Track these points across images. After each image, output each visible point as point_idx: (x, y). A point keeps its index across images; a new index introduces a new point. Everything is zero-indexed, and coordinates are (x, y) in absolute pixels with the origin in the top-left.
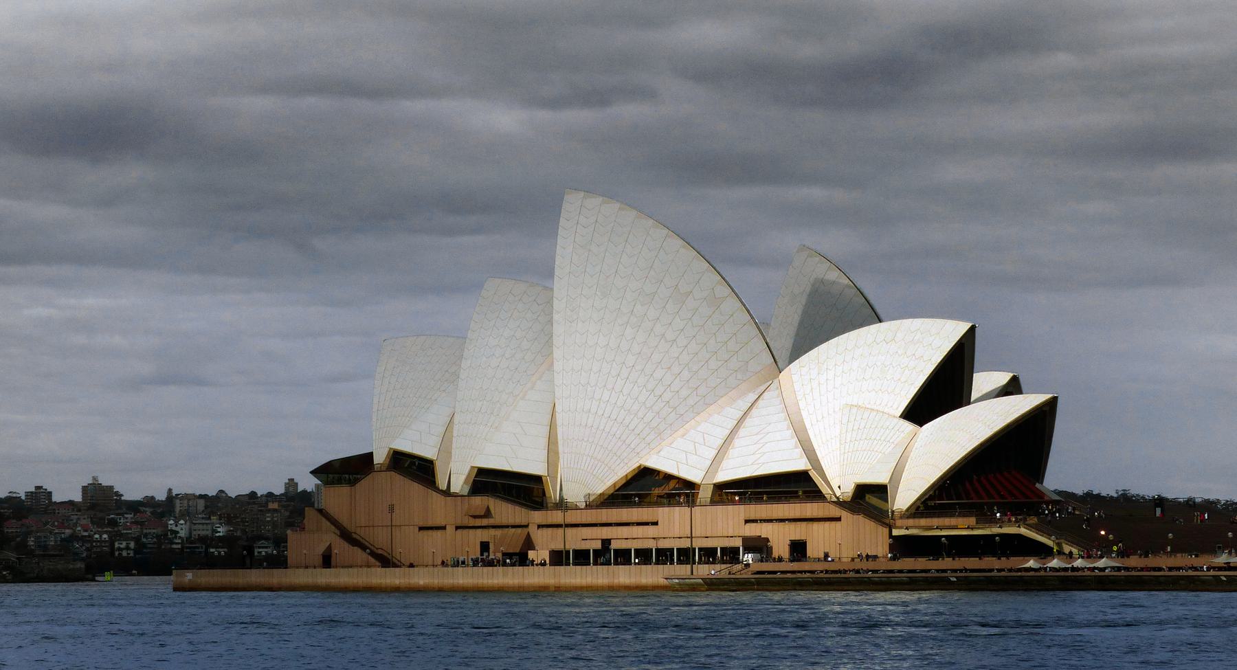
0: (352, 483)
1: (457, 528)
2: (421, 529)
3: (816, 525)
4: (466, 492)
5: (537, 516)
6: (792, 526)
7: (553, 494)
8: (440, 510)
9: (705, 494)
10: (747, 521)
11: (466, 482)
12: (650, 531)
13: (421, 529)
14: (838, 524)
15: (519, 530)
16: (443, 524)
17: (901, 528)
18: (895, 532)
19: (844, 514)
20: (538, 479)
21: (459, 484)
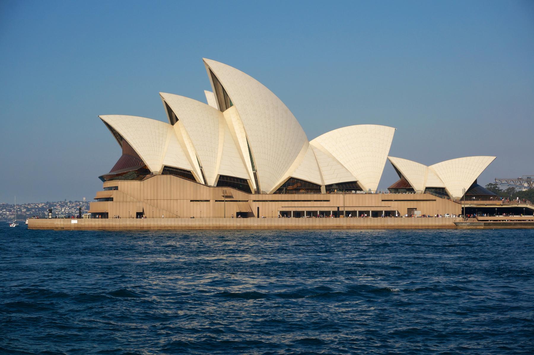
0: (141, 179)
1: (216, 201)
2: (191, 201)
3: (422, 202)
4: (216, 186)
5: (253, 197)
6: (409, 202)
7: (253, 186)
8: (205, 193)
9: (323, 189)
10: (382, 201)
11: (215, 181)
12: (325, 204)
13: (191, 201)
14: (434, 202)
15: (244, 203)
16: (208, 199)
17: (468, 204)
18: (463, 206)
19: (438, 199)
20: (245, 181)
21: (212, 181)
